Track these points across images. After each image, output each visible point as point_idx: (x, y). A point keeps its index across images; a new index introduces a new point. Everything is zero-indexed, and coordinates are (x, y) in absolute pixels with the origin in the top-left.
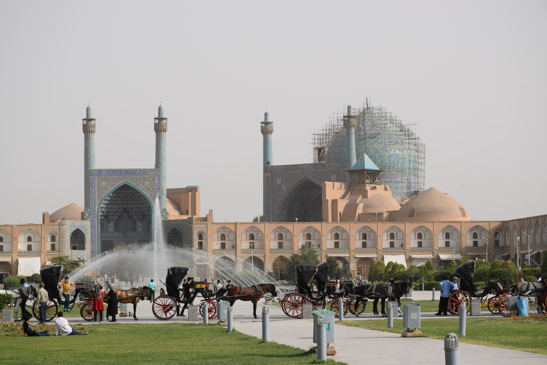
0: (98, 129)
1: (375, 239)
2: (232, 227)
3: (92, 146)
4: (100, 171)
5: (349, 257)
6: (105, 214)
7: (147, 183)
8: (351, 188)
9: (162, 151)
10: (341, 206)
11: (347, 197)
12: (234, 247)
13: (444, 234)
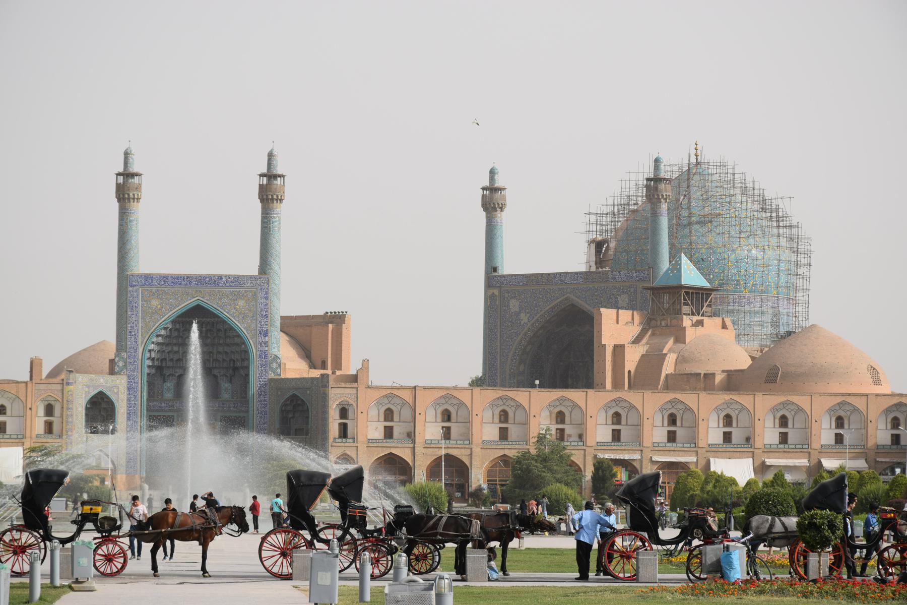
0: (146, 193)
1: (694, 426)
2: (407, 396)
3: (134, 227)
4: (148, 279)
5: (641, 461)
6: (156, 363)
7: (241, 303)
8: (653, 322)
9: (273, 241)
10: (632, 358)
11: (644, 341)
12: (411, 436)
13: (834, 419)
